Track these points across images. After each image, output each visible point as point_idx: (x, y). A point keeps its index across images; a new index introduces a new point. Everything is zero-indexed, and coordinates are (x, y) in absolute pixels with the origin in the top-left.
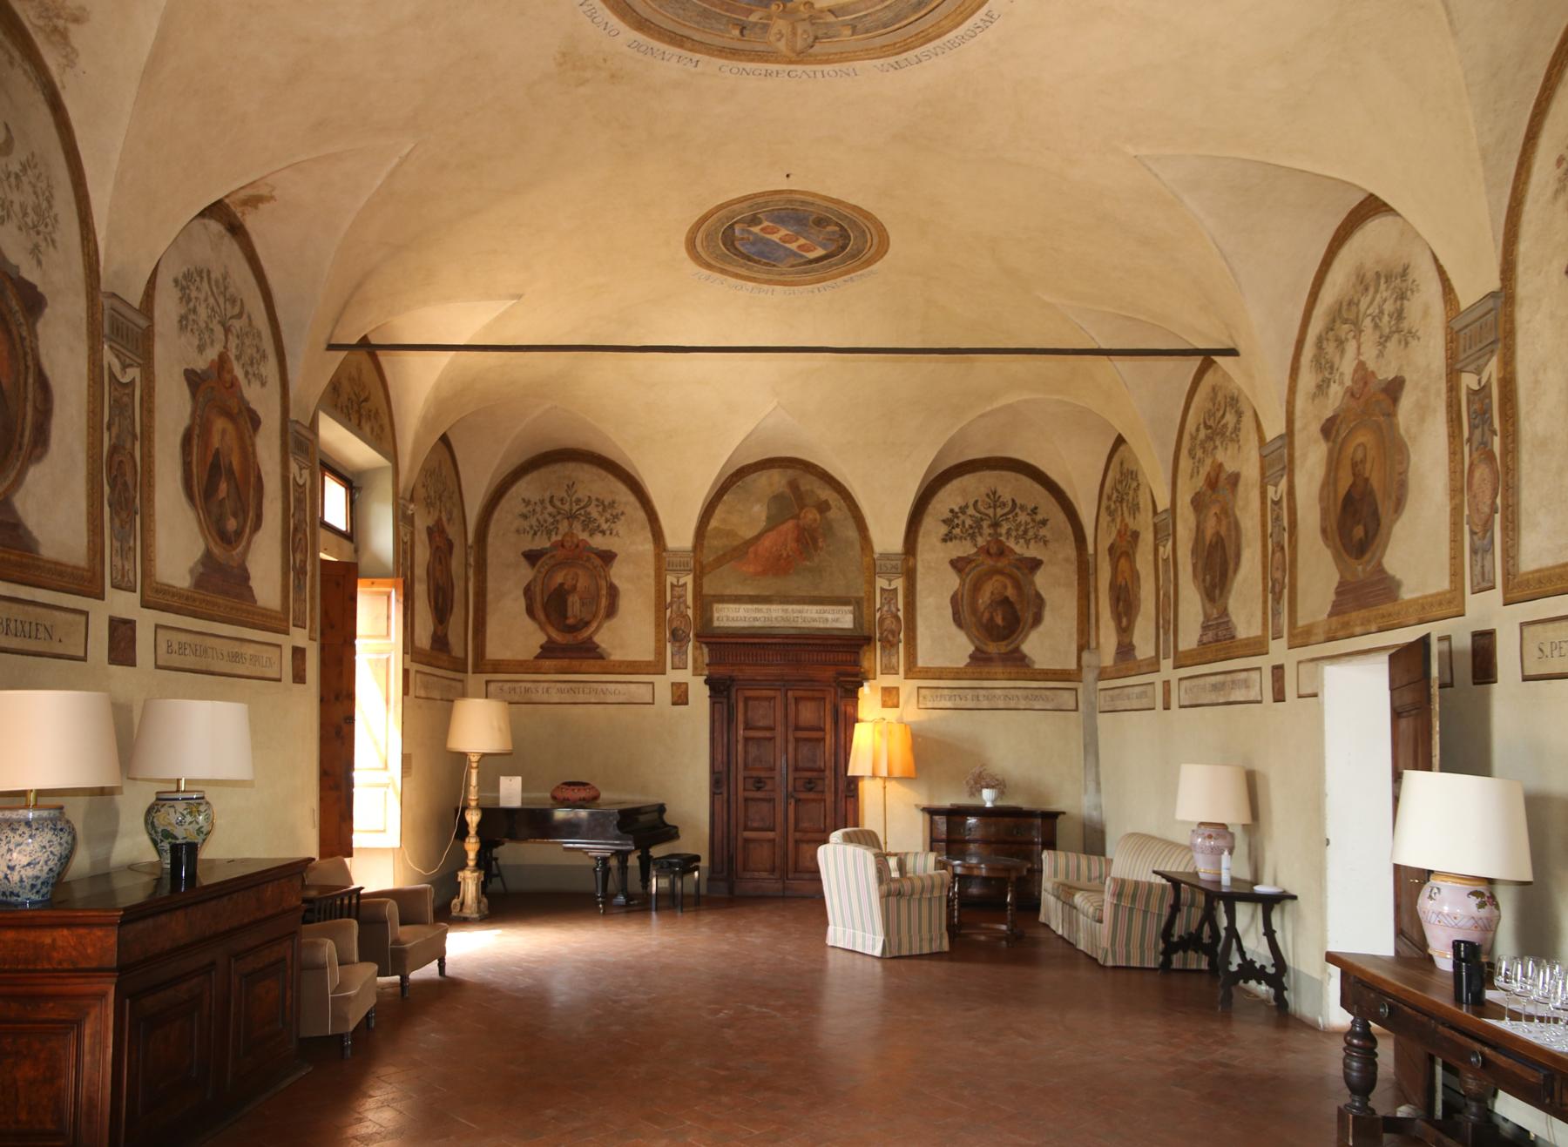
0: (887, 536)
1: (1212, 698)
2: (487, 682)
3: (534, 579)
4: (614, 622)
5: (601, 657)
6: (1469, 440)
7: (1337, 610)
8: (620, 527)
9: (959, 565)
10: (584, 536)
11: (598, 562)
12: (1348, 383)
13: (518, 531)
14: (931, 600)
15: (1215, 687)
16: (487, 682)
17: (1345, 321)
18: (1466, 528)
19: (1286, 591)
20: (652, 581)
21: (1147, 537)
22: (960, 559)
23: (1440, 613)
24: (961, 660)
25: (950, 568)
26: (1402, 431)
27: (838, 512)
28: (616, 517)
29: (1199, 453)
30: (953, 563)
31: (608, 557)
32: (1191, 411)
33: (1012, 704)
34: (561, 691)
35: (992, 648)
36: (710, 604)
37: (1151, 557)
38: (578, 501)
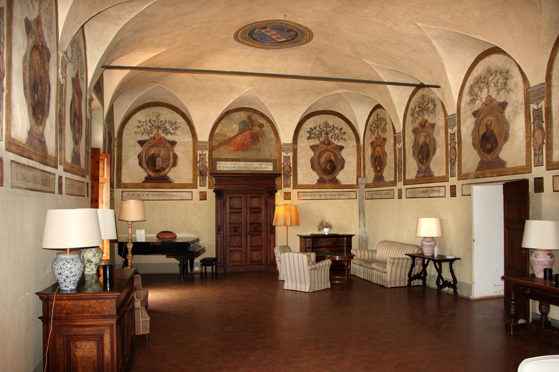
0: (286, 137)
1: (423, 195)
2: (122, 192)
3: (142, 151)
4: (175, 168)
5: (171, 182)
6: (533, 123)
7: (479, 169)
8: (178, 132)
9: (314, 148)
10: (163, 135)
11: (169, 145)
12: (484, 100)
13: (136, 133)
14: (303, 160)
15: (423, 192)
16: (122, 192)
17: (483, 83)
18: (532, 148)
19: (457, 162)
20: (192, 153)
21: (390, 141)
22: (314, 146)
23: (522, 172)
24: (315, 182)
25: (310, 149)
26: (506, 118)
27: (267, 128)
28: (177, 128)
29: (416, 115)
30: (311, 147)
31: (173, 143)
32: (412, 101)
33: (333, 197)
34: (154, 195)
35: (326, 177)
36: (216, 162)
37: (392, 148)
38: (161, 122)
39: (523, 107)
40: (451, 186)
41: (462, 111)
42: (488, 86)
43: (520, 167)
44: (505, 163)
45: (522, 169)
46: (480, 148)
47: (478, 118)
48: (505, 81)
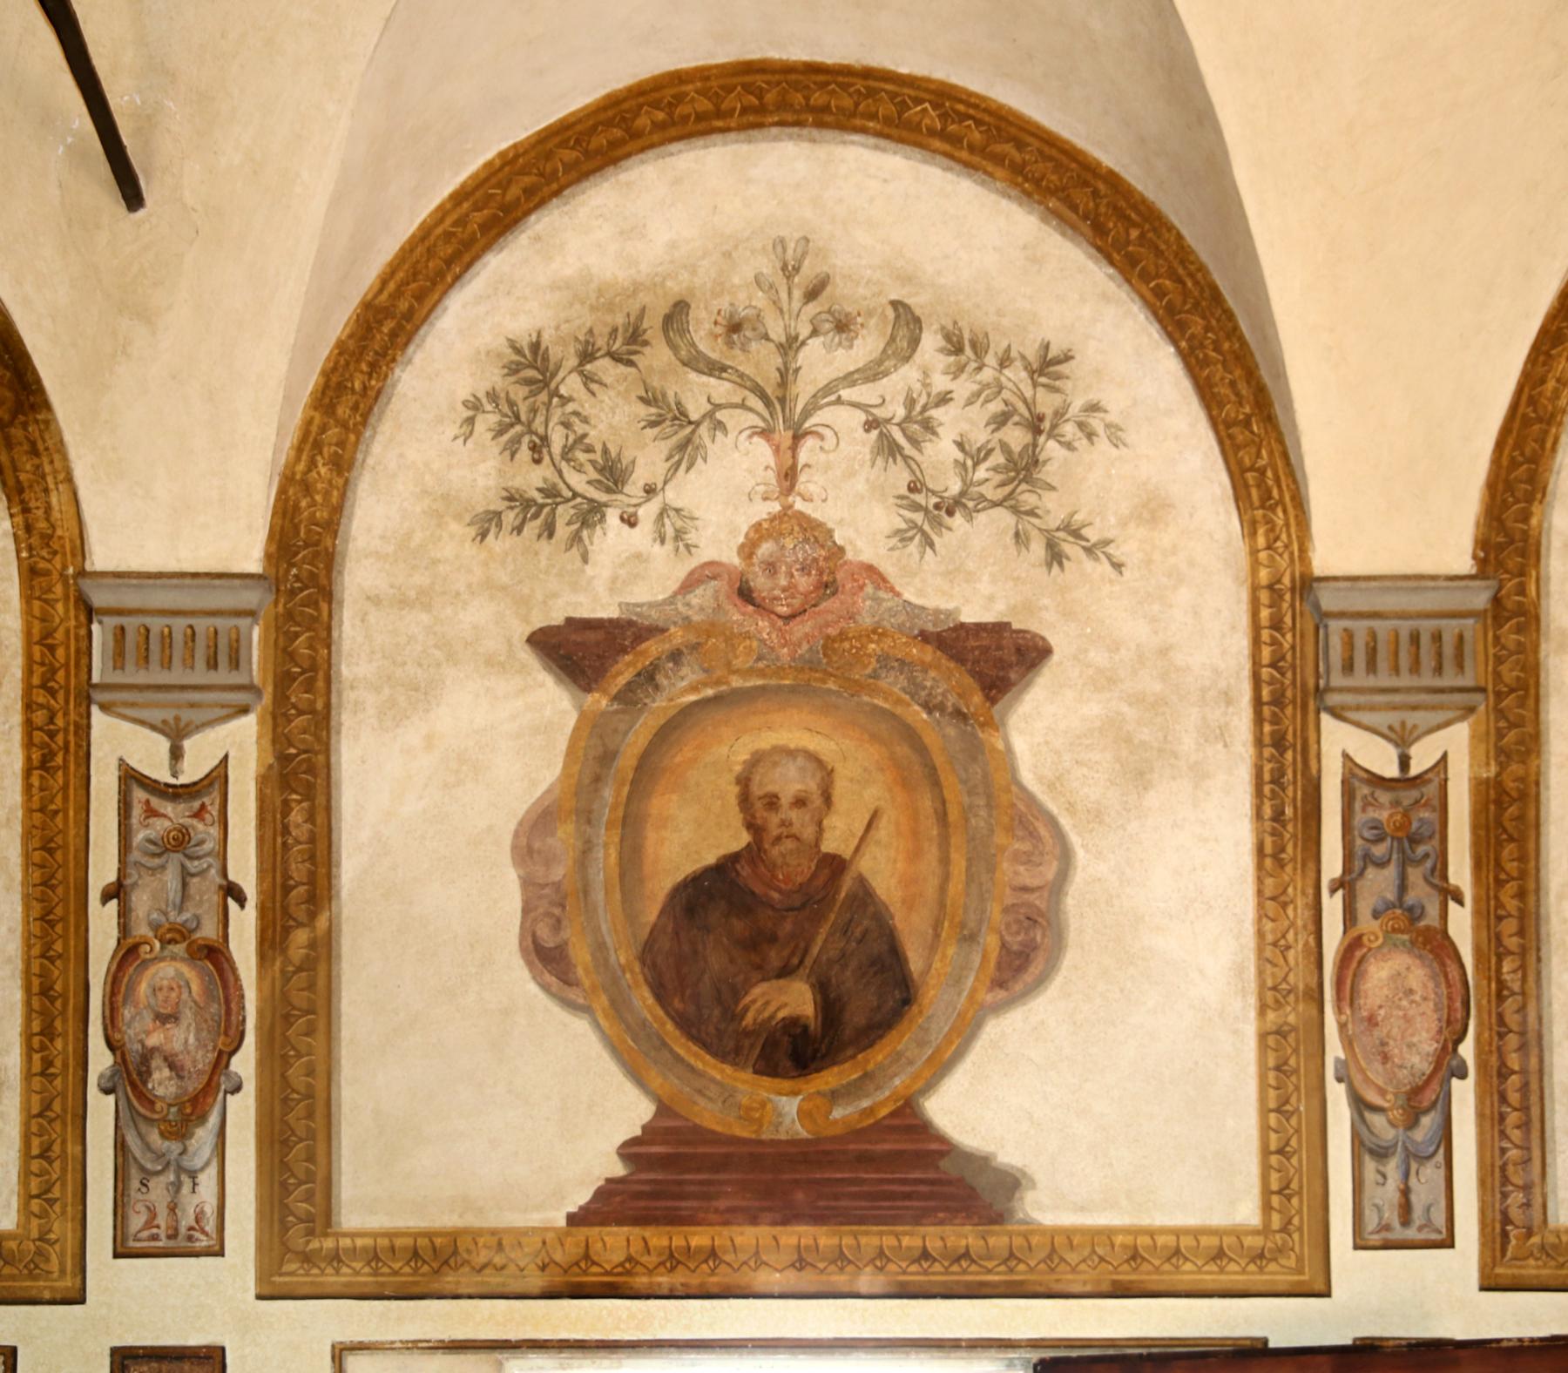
6: (1344, 884)
7: (608, 1206)
12: (719, 541)
17: (716, 369)
18: (1337, 1094)
26: (1027, 777)
41: (361, 575)
42: (786, 420)
44: (1012, 1182)
45: (1219, 1255)
46: (643, 1000)
47: (628, 698)
48: (1016, 437)
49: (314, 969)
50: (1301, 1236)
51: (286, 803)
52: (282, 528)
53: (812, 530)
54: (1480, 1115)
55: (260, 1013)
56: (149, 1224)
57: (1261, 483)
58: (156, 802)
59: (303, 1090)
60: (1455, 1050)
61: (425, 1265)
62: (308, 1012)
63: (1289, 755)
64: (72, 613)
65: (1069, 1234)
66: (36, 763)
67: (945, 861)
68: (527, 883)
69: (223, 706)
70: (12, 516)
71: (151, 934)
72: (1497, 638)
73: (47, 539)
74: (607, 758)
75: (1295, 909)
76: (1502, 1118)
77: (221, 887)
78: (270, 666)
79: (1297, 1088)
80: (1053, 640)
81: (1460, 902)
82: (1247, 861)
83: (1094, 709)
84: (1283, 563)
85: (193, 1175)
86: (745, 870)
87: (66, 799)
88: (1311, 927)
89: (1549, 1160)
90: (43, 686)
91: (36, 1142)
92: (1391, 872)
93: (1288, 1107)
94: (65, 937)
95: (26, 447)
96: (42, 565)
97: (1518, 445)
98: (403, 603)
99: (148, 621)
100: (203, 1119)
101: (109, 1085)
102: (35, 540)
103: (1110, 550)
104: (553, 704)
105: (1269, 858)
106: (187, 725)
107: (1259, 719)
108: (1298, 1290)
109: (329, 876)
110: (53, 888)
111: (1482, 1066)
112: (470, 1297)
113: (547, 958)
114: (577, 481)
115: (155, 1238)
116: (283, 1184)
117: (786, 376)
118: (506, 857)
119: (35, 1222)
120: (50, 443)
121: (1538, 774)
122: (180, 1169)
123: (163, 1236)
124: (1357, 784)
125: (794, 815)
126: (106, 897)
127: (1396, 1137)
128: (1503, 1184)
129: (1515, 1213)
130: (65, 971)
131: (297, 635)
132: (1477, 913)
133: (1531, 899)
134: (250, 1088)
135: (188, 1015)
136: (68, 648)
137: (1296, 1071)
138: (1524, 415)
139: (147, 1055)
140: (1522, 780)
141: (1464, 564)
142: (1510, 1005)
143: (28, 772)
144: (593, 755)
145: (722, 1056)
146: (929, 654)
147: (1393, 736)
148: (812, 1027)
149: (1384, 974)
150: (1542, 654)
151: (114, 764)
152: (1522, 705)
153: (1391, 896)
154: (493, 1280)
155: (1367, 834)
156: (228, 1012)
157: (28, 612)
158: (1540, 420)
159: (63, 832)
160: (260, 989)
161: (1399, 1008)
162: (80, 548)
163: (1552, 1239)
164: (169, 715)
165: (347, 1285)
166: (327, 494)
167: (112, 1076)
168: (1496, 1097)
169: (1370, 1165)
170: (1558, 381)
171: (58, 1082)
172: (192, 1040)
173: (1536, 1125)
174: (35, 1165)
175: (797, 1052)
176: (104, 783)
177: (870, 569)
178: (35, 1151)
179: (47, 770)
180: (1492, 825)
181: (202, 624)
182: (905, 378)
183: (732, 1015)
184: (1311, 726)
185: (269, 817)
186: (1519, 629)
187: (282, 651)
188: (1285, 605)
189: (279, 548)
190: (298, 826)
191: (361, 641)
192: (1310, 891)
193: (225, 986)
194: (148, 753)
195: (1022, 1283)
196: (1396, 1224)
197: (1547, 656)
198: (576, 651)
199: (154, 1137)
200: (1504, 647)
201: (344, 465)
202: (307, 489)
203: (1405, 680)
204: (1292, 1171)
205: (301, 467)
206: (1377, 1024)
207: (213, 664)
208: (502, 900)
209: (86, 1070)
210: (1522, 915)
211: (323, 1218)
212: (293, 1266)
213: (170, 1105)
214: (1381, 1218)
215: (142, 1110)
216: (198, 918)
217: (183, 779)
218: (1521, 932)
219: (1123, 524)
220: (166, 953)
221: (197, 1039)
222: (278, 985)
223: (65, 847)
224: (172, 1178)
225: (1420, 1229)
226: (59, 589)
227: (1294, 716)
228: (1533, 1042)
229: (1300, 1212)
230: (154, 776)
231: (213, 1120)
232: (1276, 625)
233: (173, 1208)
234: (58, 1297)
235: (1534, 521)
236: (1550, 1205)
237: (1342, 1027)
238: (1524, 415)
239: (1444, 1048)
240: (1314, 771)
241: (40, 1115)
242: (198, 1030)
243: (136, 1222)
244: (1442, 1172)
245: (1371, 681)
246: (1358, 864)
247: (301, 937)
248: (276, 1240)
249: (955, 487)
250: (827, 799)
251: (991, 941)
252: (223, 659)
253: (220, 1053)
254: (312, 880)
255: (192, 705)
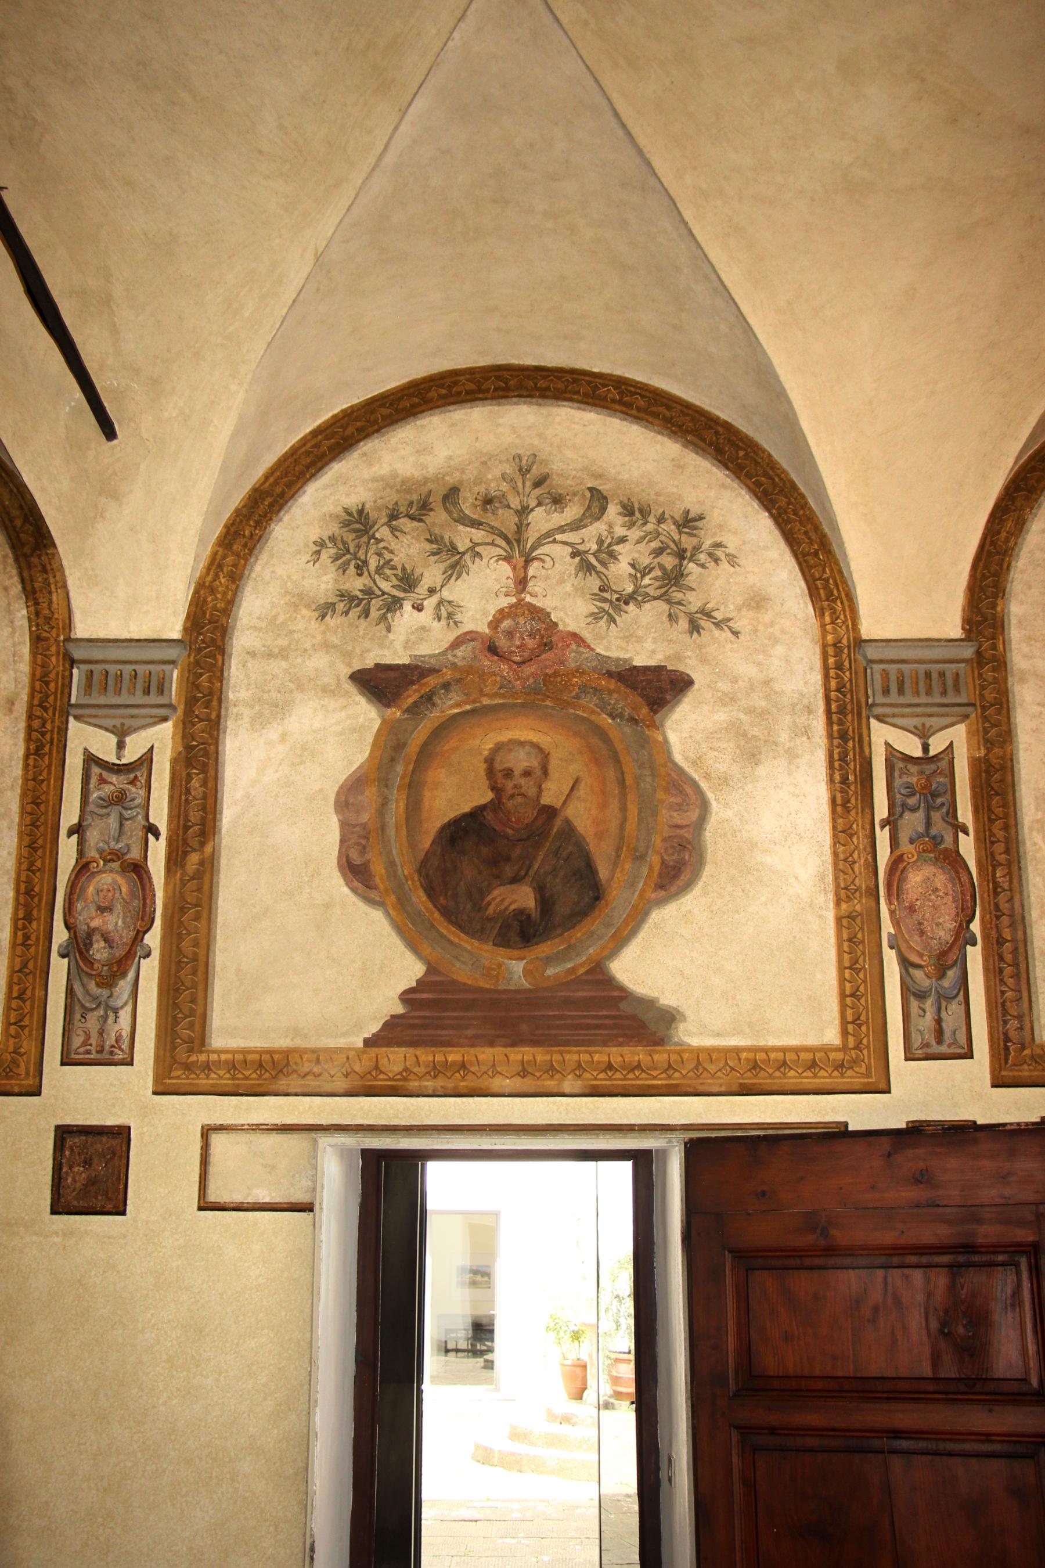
7: (392, 1033)
17: (475, 524)
18: (890, 956)
19: (150, 970)
26: (678, 758)
39: (819, 724)
40: (63, 1133)
41: (243, 640)
42: (519, 549)
43: (797, 1050)
44: (670, 1017)
45: (813, 1065)
46: (419, 898)
47: (414, 710)
48: (668, 561)
49: (202, 878)
50: (869, 1051)
51: (189, 775)
52: (195, 613)
53: (538, 614)
54: (986, 970)
55: (165, 907)
56: (85, 1043)
57: (826, 586)
58: (105, 774)
59: (190, 956)
60: (968, 927)
61: (264, 1072)
62: (196, 906)
63: (850, 744)
64: (61, 663)
65: (710, 1053)
66: (32, 751)
67: (623, 809)
68: (344, 825)
69: (151, 717)
70: (27, 607)
71: (98, 856)
72: (980, 675)
73: (48, 620)
74: (399, 747)
75: (858, 838)
76: (1001, 971)
77: (144, 827)
78: (184, 693)
79: (863, 953)
80: (694, 676)
81: (967, 834)
82: (825, 809)
83: (722, 716)
84: (842, 632)
85: (116, 1011)
86: (489, 816)
87: (49, 773)
88: (869, 849)
89: (1033, 999)
90: (40, 705)
91: (16, 988)
92: (921, 814)
93: (857, 966)
94: (43, 857)
95: (40, 568)
96: (45, 634)
97: (985, 567)
98: (270, 655)
99: (107, 667)
100: (124, 974)
101: (65, 952)
102: (41, 621)
103: (730, 624)
104: (366, 715)
105: (839, 806)
106: (129, 728)
107: (830, 722)
108: (868, 1089)
109: (214, 820)
110: (37, 827)
111: (986, 937)
112: (296, 1095)
113: (356, 871)
114: (385, 586)
115: (88, 1052)
116: (175, 1017)
117: (521, 528)
118: (331, 808)
119: (12, 1041)
120: (55, 566)
121: (1012, 754)
122: (108, 1007)
123: (94, 1052)
124: (895, 761)
125: (523, 781)
126: (70, 833)
127: (931, 985)
128: (1004, 1015)
129: (1012, 1034)
130: (42, 880)
131: (201, 675)
132: (977, 840)
133: (1013, 831)
134: (156, 954)
135: (118, 908)
136: (57, 682)
137: (862, 942)
138: (988, 551)
139: (90, 933)
140: (1002, 758)
141: (957, 633)
142: (1002, 898)
143: (27, 756)
144: (390, 746)
145: (472, 934)
146: (613, 684)
147: (917, 732)
148: (533, 915)
149: (918, 879)
150: (1010, 684)
151: (81, 751)
152: (999, 714)
153: (921, 829)
154: (312, 1083)
155: (903, 791)
156: (145, 904)
157: (34, 662)
158: (998, 553)
159: (47, 793)
160: (166, 891)
161: (929, 900)
162: (69, 625)
163: (1038, 1051)
164: (117, 722)
165: (213, 1085)
166: (225, 594)
167: (67, 946)
168: (996, 957)
169: (914, 1004)
170: (1008, 532)
171: (32, 950)
172: (120, 923)
173: (1024, 976)
174: (14, 1004)
175: (522, 932)
176: (74, 763)
177: (575, 636)
178: (15, 994)
179: (38, 755)
180: (984, 786)
181: (141, 669)
182: (598, 528)
183: (479, 907)
184: (864, 726)
185: (178, 783)
186: (994, 669)
187: (192, 684)
188: (844, 656)
189: (192, 624)
190: (196, 789)
191: (242, 678)
192: (868, 827)
193: (143, 889)
194: (102, 744)
195: (677, 1085)
196: (933, 1042)
197: (1013, 685)
198: (379, 684)
199: (92, 986)
200: (985, 680)
201: (236, 578)
202: (212, 590)
203: (923, 699)
204: (861, 1008)
205: (209, 578)
206: (915, 911)
207: (147, 692)
208: (329, 833)
209: (51, 942)
210: (1007, 841)
211: (200, 1040)
212: (179, 1073)
213: (104, 965)
214: (923, 1040)
215: (85, 969)
216: (128, 846)
217: (124, 761)
218: (1007, 851)
219: (739, 610)
220: (107, 868)
221: (124, 923)
222: (178, 889)
223: (47, 802)
224: (102, 1013)
225: (949, 1046)
226: (54, 649)
227: (853, 720)
228: (1019, 922)
229: (867, 1035)
230: (106, 759)
231: (131, 975)
232: (839, 667)
233: (101, 1033)
234: (23, 1090)
235: (999, 609)
236: (1036, 1028)
237: (892, 913)
238: (988, 551)
239: (961, 926)
240: (867, 754)
241: (20, 971)
242: (124, 918)
243: (77, 1041)
244: (963, 1007)
245: (901, 700)
246: (898, 810)
247: (194, 858)
248: (168, 1055)
249: (629, 588)
250: (545, 772)
251: (655, 860)
252: (153, 689)
253: (138, 931)
254: (203, 822)
255: (132, 717)
